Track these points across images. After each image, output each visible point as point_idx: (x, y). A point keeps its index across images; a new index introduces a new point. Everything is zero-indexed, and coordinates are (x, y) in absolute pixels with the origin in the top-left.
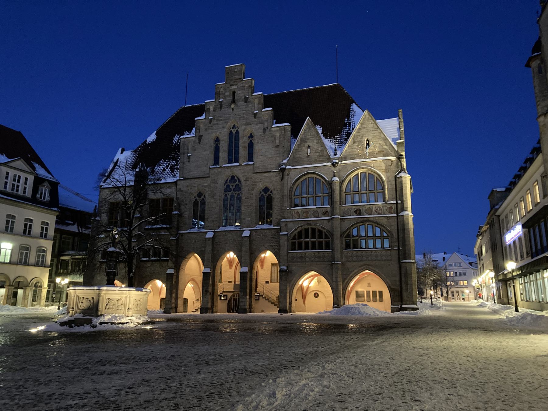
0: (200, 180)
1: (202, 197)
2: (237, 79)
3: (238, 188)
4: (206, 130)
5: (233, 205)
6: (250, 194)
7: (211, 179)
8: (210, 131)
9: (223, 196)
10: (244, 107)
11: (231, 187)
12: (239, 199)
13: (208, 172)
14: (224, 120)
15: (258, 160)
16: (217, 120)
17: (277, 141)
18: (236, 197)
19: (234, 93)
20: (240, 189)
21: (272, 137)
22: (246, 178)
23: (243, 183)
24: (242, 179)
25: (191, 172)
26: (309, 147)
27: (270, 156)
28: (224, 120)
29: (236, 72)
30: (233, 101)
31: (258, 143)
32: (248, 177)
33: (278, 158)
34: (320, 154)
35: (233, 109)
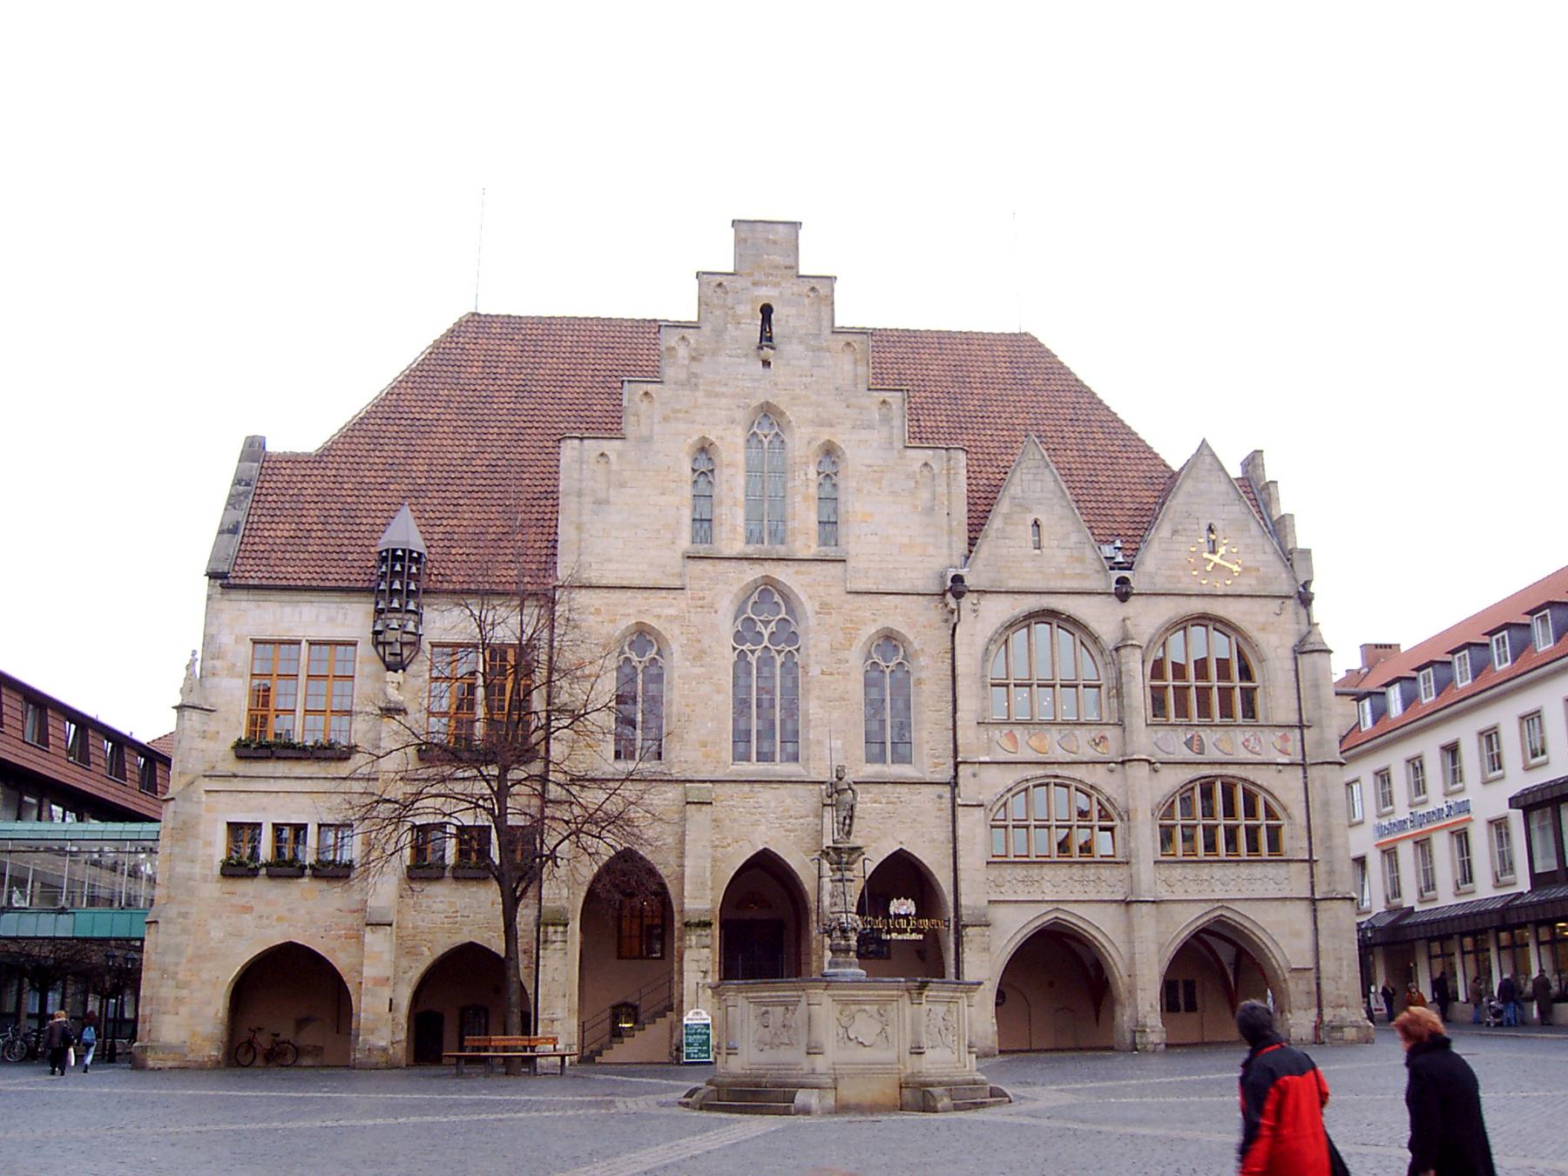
0: (647, 593)
1: (652, 653)
2: (776, 267)
3: (788, 634)
4: (666, 419)
5: (771, 692)
6: (839, 661)
7: (688, 593)
8: (682, 426)
9: (734, 656)
10: (805, 363)
11: (760, 627)
12: (791, 667)
13: (678, 570)
14: (734, 396)
15: (859, 541)
16: (708, 394)
17: (925, 495)
18: (778, 664)
19: (767, 311)
20: (793, 638)
21: (909, 476)
22: (823, 605)
23: (812, 621)
24: (809, 606)
25: (609, 560)
26: (1036, 524)
27: (906, 540)
28: (734, 396)
29: (775, 243)
30: (766, 337)
31: (859, 491)
32: (828, 599)
33: (931, 551)
34: (1076, 553)
35: (766, 363)
